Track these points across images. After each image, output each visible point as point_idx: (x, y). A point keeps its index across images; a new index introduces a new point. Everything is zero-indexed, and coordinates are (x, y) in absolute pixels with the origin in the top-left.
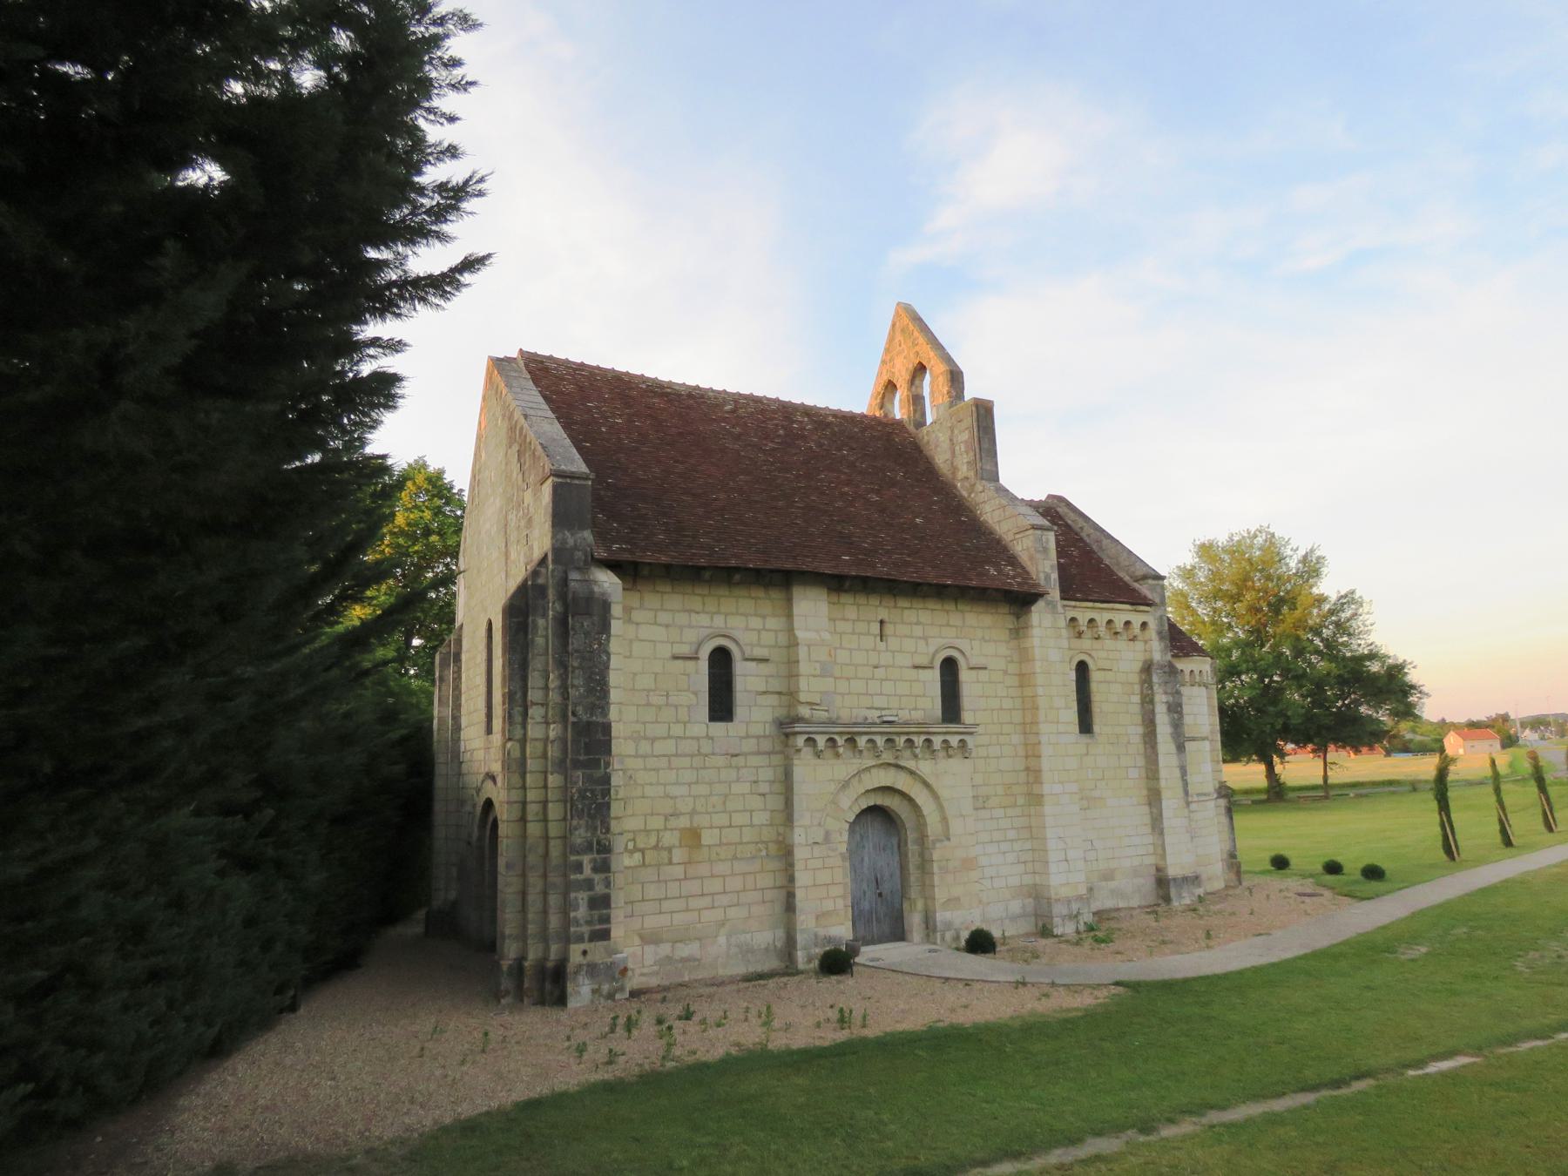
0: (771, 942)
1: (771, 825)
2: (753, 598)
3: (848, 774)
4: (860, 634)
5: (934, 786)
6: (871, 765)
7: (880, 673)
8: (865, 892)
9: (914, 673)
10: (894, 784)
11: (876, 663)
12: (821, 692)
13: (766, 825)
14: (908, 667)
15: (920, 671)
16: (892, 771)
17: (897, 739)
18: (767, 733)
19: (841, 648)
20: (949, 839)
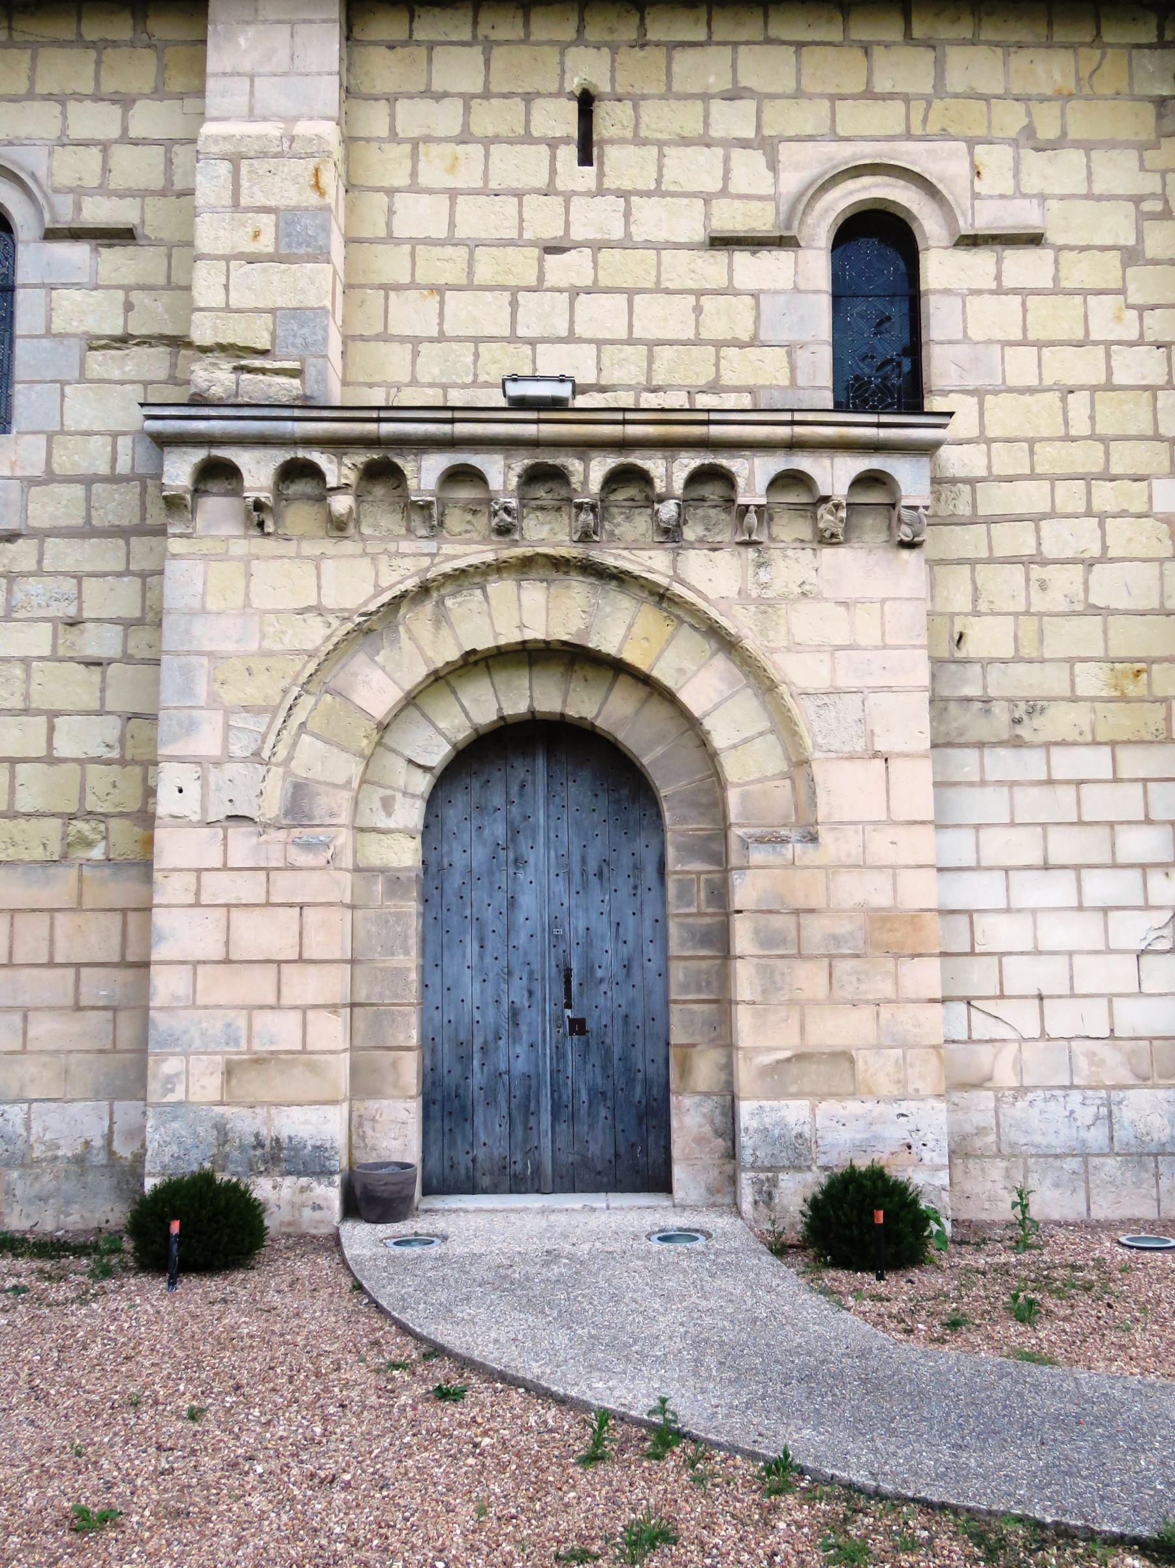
0: (98, 1142)
1: (123, 762)
2: (92, 45)
3: (379, 591)
4: (488, 142)
5: (751, 643)
6: (475, 560)
8: (514, 1014)
9: (714, 266)
10: (587, 631)
11: (552, 231)
12: (272, 311)
13: (109, 762)
14: (691, 247)
15: (742, 257)
16: (578, 590)
17: (574, 465)
19: (414, 188)
20: (813, 839)
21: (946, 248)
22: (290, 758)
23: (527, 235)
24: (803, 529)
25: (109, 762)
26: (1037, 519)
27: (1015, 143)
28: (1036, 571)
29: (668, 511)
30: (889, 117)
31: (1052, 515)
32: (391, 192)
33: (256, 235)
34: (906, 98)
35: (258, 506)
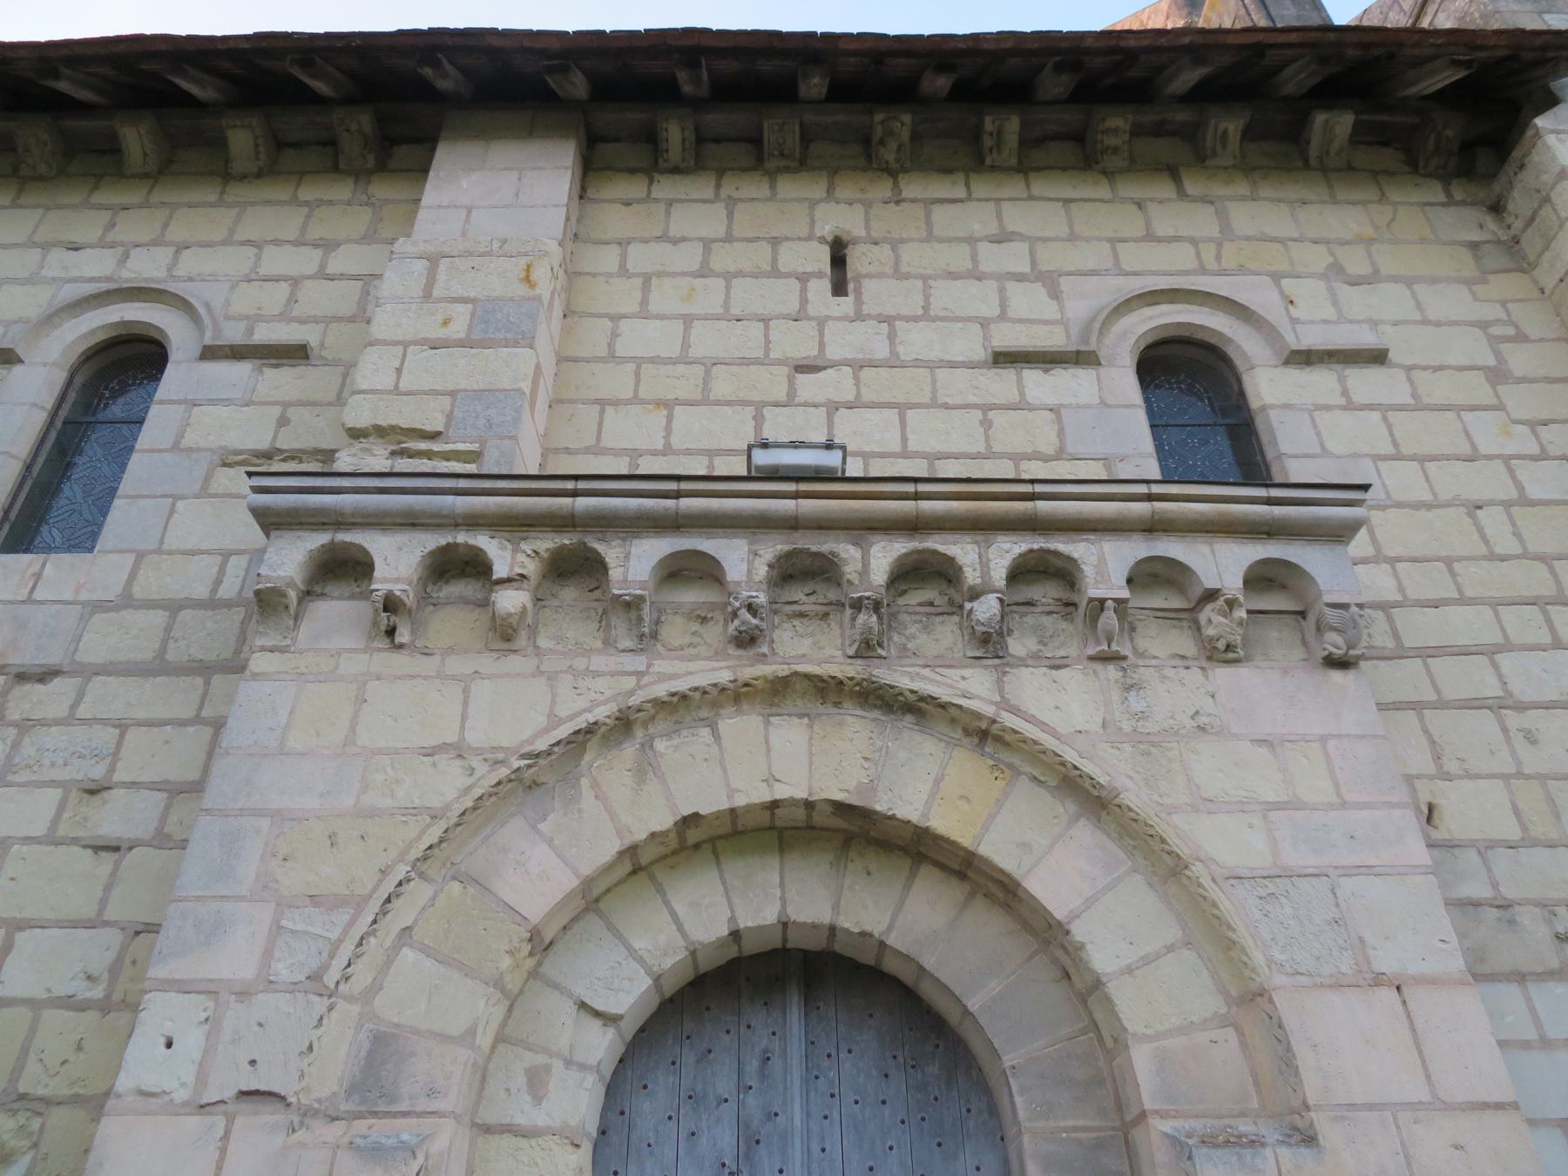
2: (307, 203)
3: (554, 721)
5: (1134, 796)
6: (702, 681)
7: (834, 385)
9: (1002, 384)
10: (871, 787)
11: (806, 349)
12: (453, 394)
13: (82, 1006)
14: (971, 365)
17: (847, 552)
18: (228, 590)
19: (644, 314)
21: (1276, 366)
22: (375, 988)
23: (773, 355)
24: (1181, 641)
25: (82, 1006)
26: (1490, 652)
27: (1324, 277)
28: (1513, 719)
29: (986, 609)
30: (1182, 257)
31: (1507, 646)
32: (616, 318)
33: (446, 323)
34: (1193, 241)
35: (391, 605)
